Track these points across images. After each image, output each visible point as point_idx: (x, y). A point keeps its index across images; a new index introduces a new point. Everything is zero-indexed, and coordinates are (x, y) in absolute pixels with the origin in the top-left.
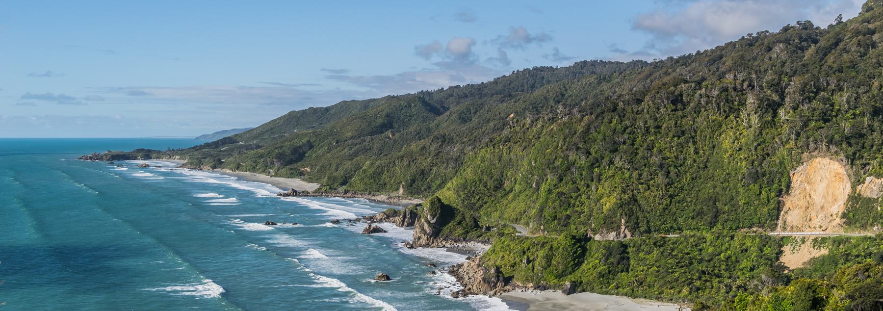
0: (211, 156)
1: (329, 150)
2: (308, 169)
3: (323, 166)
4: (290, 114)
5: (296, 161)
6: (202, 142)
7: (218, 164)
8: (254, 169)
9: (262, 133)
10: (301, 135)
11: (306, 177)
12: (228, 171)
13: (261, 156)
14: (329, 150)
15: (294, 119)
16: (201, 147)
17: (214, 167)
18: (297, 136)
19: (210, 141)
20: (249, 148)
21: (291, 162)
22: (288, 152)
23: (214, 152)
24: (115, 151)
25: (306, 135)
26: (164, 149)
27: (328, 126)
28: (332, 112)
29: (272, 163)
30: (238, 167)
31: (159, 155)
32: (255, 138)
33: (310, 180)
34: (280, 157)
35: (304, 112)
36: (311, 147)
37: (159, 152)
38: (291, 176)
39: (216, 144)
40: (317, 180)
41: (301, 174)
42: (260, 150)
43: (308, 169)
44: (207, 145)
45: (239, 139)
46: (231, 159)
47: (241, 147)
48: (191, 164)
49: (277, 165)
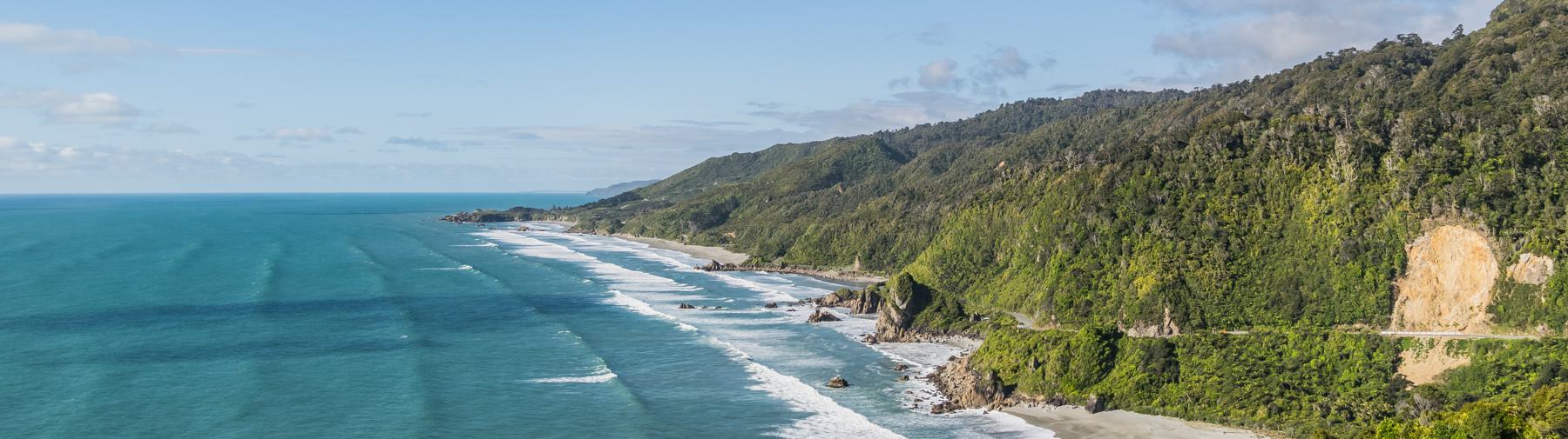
0: (609, 217)
1: (760, 209)
2: (733, 235)
3: (752, 231)
4: (708, 162)
5: (718, 224)
6: (597, 198)
7: (616, 227)
8: (662, 234)
9: (674, 187)
10: (722, 189)
11: (731, 245)
12: (630, 236)
13: (672, 217)
14: (760, 209)
15: (714, 168)
16: (595, 205)
17: (612, 232)
18: (719, 190)
19: (606, 197)
20: (657, 206)
21: (710, 225)
22: (707, 212)
23: (612, 211)
24: (487, 210)
25: (730, 189)
26: (547, 208)
27: (758, 178)
28: (762, 159)
29: (686, 226)
30: (643, 231)
31: (542, 214)
32: (662, 194)
33: (736, 250)
34: (697, 218)
35: (726, 159)
36: (737, 205)
37: (542, 211)
38: (711, 244)
39: (614, 202)
40: (745, 249)
41: (724, 241)
42: (671, 210)
43: (733, 235)
44: (603, 202)
45: (642, 194)
46: (634, 220)
47: (646, 204)
48: (582, 226)
49: (693, 228)
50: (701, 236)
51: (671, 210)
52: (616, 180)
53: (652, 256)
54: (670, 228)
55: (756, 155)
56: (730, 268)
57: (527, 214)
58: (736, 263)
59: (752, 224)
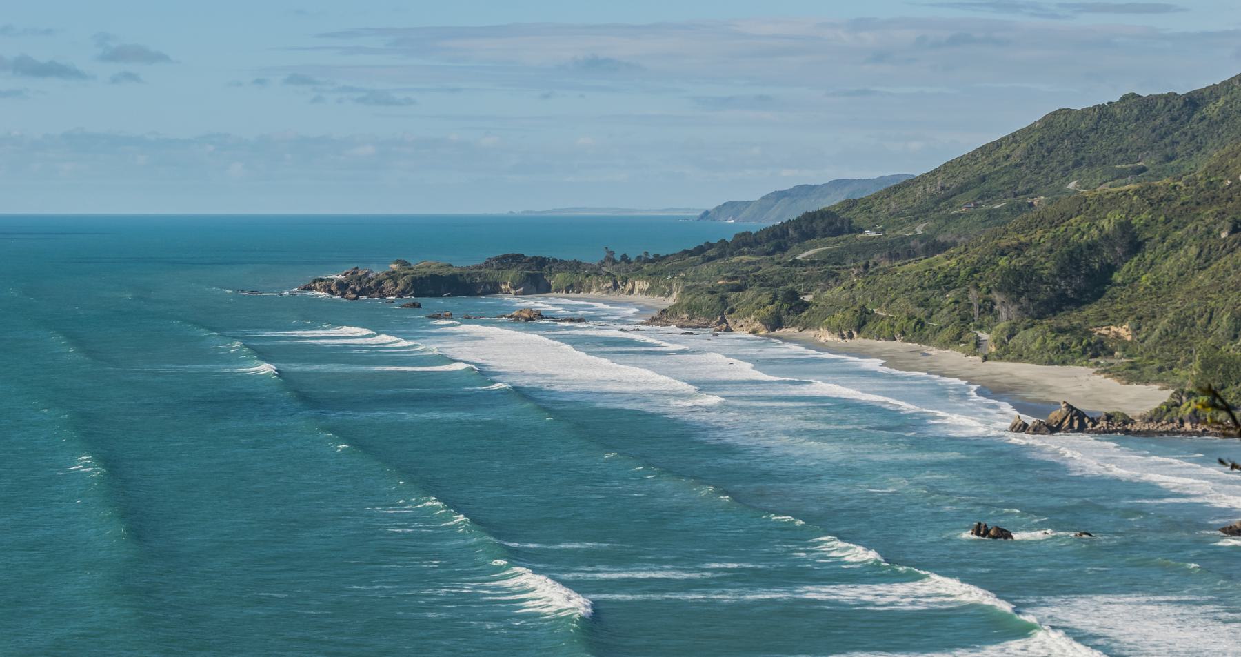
0: (764, 281)
1: (1205, 260)
2: (1124, 331)
3: (1182, 322)
4: (1049, 122)
5: (1079, 301)
6: (732, 226)
7: (787, 311)
8: (918, 330)
9: (948, 196)
10: (1095, 199)
11: (1119, 359)
12: (825, 336)
13: (948, 282)
14: (1205, 260)
15: (1065, 140)
16: (724, 249)
17: (775, 323)
18: (1081, 205)
19: (755, 226)
20: (901, 250)
21: (1058, 304)
22: (1049, 267)
23: (775, 266)
24: (426, 263)
25: (1114, 200)
26: (592, 257)
27: (1199, 166)
28: (1212, 110)
29: (988, 308)
30: (862, 322)
31: (578, 275)
32: (920, 213)
33: (1133, 374)
34: (1019, 284)
35: (1103, 112)
36: (1136, 247)
37: (575, 266)
38: (1062, 356)
39: (778, 239)
40: (1162, 373)
41: (1097, 350)
42: (943, 262)
43: (1124, 331)
44: (746, 242)
45: (859, 218)
46: (836, 292)
47: (868, 248)
48: (692, 309)
49: (1007, 313)
50: (1029, 337)
51: (943, 262)
52: (788, 179)
53: (743, 393)
54: (942, 312)
55: (1193, 102)
56: (1116, 426)
57: (536, 275)
58: (1134, 411)
59: (1179, 300)
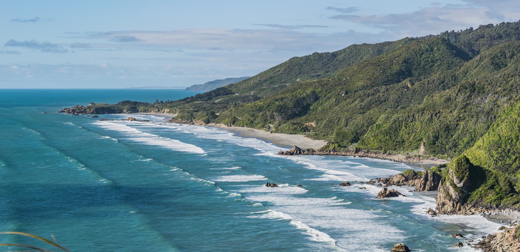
0: (204, 109)
1: (337, 103)
2: (313, 124)
3: (330, 121)
5: (300, 115)
6: (194, 93)
7: (211, 118)
8: (251, 124)
9: (261, 83)
10: (305, 84)
11: (312, 133)
12: (223, 126)
13: (260, 109)
14: (337, 103)
15: (296, 66)
16: (193, 99)
17: (207, 122)
18: (301, 86)
19: (202, 92)
20: (246, 99)
21: (294, 116)
22: (291, 104)
23: (209, 103)
24: (100, 103)
25: (311, 84)
26: (152, 102)
27: (336, 74)
28: (340, 57)
30: (234, 122)
31: (147, 107)
32: (252, 89)
33: (316, 137)
34: (281, 110)
35: (307, 58)
36: (317, 99)
37: (146, 104)
38: (294, 132)
39: (209, 96)
40: (324, 137)
41: (305, 130)
42: (259, 103)
43: (313, 124)
44: (199, 97)
45: (234, 90)
46: (226, 112)
47: (237, 98)
48: (182, 117)
51: (259, 103)
54: (258, 118)
56: (311, 152)
58: (316, 148)
